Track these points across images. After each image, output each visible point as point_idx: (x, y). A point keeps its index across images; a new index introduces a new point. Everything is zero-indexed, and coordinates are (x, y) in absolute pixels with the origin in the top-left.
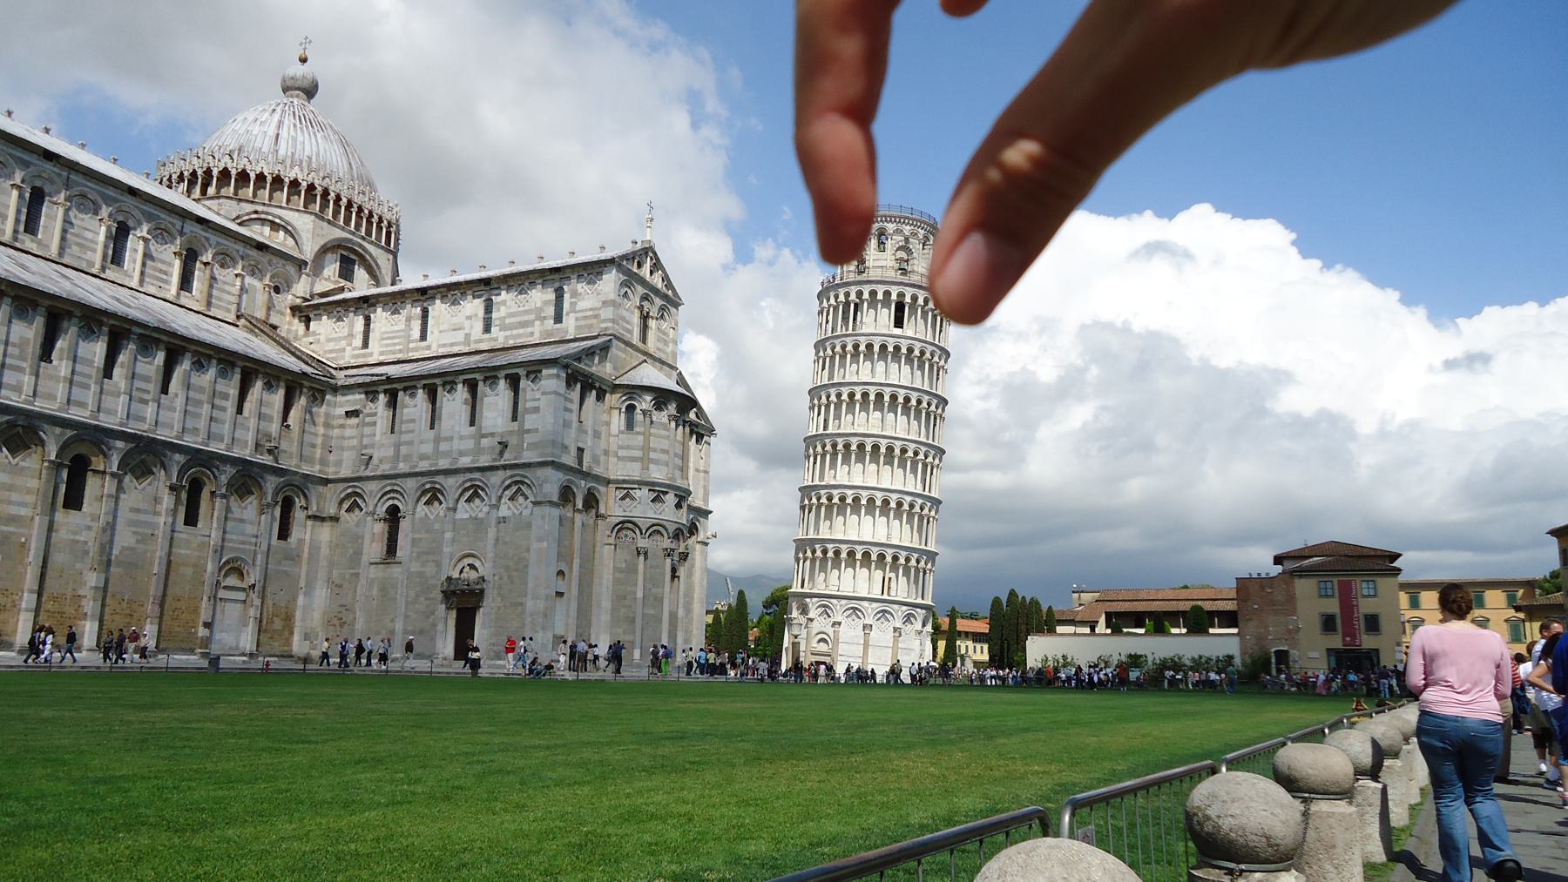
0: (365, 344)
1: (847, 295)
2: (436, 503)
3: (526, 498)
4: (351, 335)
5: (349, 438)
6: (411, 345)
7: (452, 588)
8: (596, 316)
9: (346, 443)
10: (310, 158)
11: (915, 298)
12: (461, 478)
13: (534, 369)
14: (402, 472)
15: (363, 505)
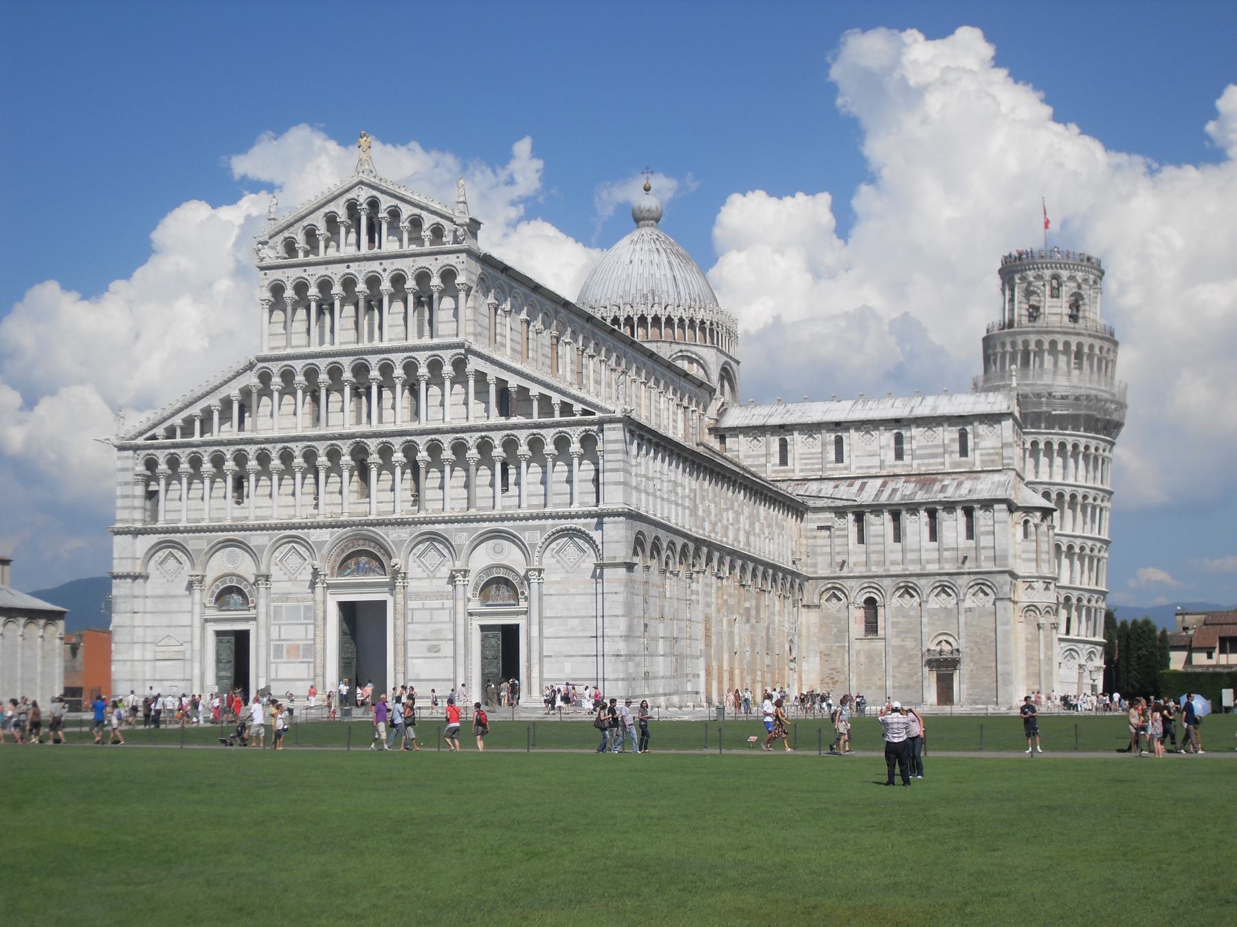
0: (783, 461)
1: (1026, 343)
2: (907, 596)
3: (986, 594)
4: (767, 455)
5: (822, 546)
6: (829, 466)
7: (931, 657)
8: (997, 454)
9: (819, 550)
10: (699, 296)
11: (1091, 347)
12: (932, 580)
13: (987, 504)
14: (878, 574)
15: (842, 596)
